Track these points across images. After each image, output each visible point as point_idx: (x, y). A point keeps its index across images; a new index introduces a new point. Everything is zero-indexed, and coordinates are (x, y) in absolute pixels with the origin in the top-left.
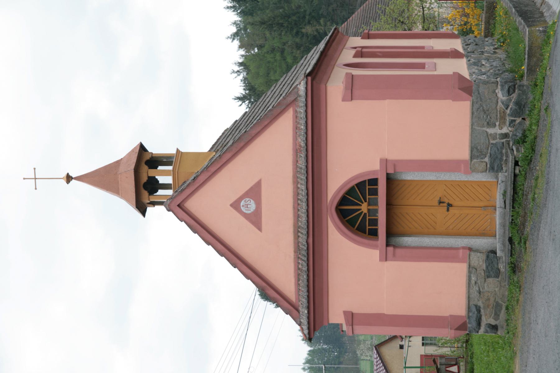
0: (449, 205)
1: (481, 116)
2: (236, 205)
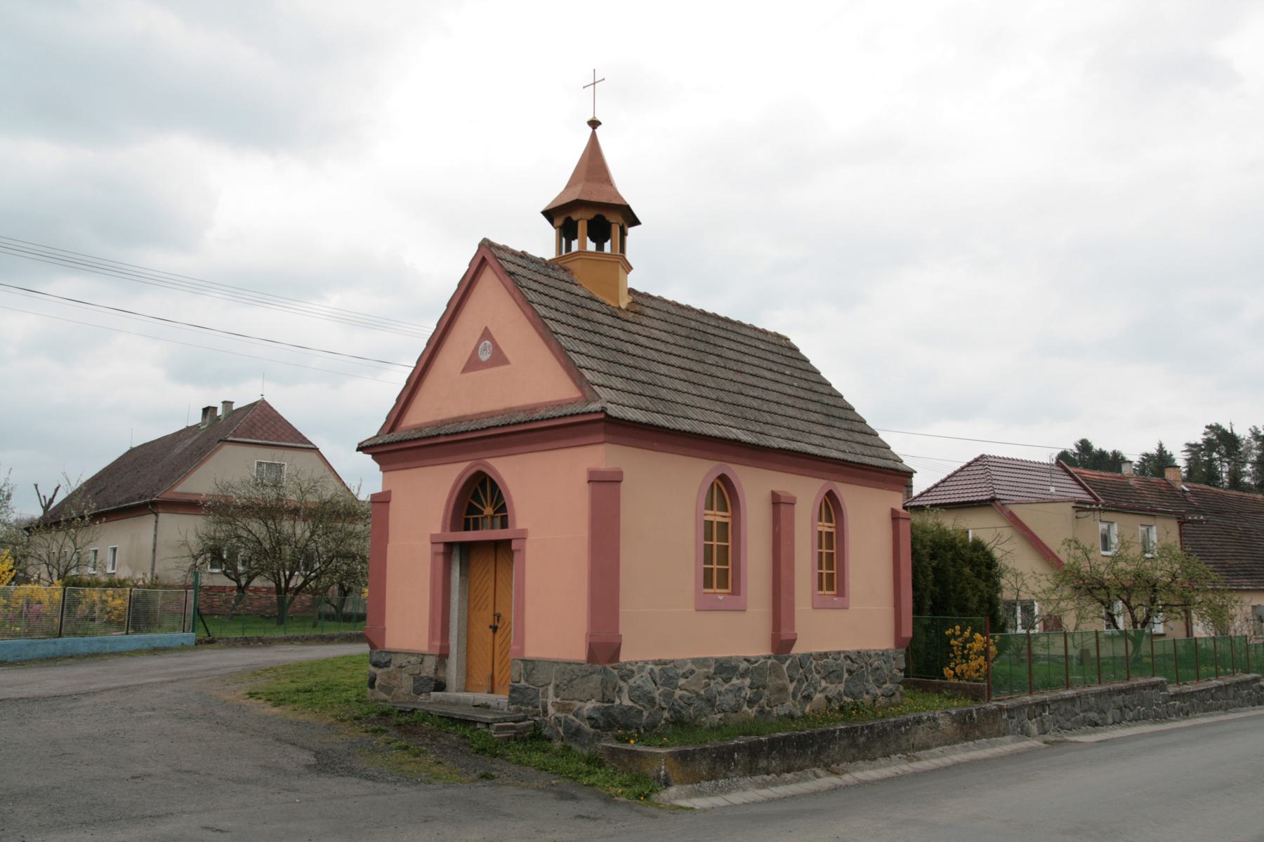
0: (495, 629)
1: (568, 675)
2: (486, 334)
